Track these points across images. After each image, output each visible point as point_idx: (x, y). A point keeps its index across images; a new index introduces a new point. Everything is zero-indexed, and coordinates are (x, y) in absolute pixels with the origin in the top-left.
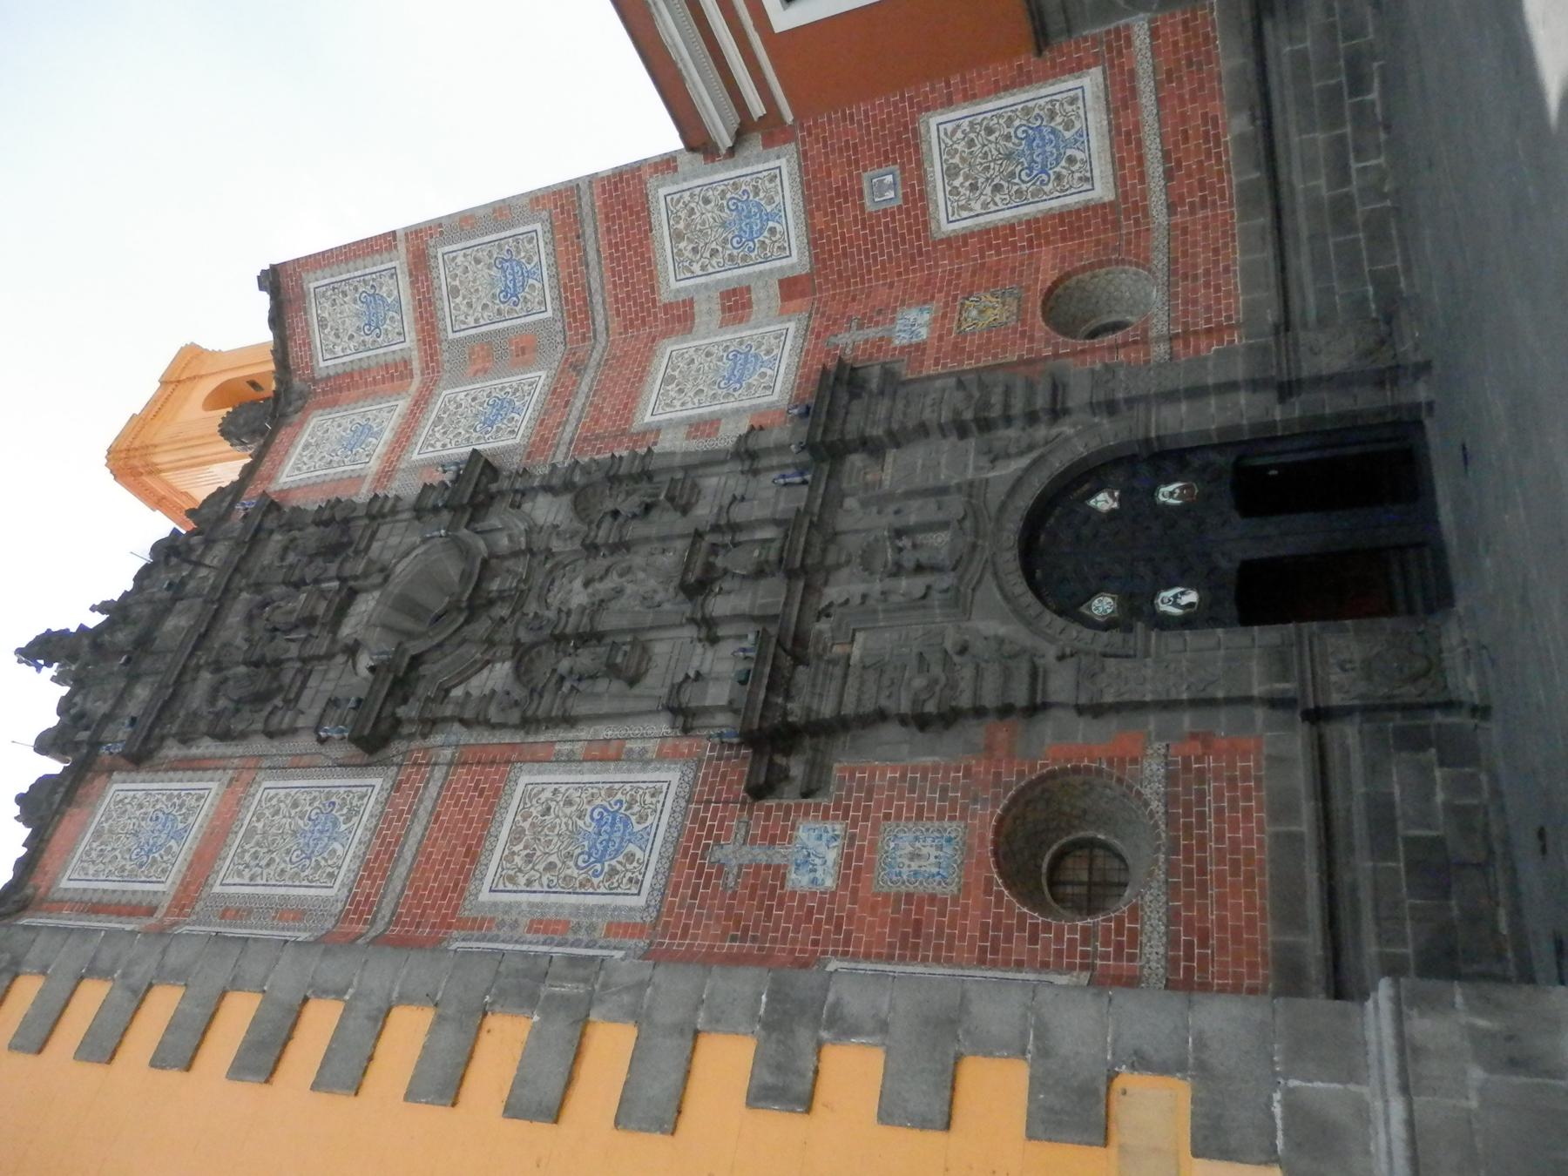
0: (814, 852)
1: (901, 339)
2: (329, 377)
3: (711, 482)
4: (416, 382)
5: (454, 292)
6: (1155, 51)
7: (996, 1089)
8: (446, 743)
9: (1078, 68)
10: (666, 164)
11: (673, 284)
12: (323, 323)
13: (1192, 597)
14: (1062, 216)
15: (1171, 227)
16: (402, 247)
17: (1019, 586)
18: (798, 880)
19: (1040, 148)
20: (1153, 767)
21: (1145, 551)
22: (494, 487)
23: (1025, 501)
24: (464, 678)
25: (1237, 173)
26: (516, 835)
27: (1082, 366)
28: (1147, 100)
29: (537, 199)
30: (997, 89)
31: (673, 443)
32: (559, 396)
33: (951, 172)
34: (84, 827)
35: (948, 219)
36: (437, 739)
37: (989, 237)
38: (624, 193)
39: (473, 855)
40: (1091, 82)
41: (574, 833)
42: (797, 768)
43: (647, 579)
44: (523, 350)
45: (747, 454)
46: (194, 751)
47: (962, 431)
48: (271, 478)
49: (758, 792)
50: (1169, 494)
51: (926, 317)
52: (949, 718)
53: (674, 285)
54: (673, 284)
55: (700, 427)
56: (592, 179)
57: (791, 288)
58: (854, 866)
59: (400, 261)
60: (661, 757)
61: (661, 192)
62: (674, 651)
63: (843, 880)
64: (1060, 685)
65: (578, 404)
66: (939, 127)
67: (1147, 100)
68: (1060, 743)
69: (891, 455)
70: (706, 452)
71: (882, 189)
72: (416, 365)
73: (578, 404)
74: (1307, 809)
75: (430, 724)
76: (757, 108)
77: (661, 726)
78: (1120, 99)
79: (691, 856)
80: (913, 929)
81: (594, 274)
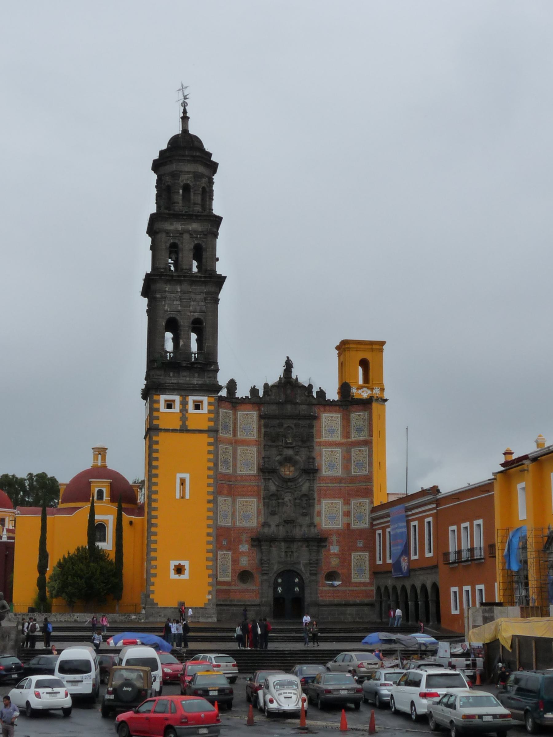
0: (244, 548)
1: (331, 547)
2: (349, 416)
3: (307, 518)
4: (346, 440)
5: (360, 451)
6: (369, 590)
7: (210, 589)
8: (262, 483)
9: (370, 578)
10: (372, 502)
11: (353, 502)
12: (359, 415)
13: (280, 592)
14: (351, 574)
15: (346, 590)
16: (370, 438)
17: (282, 570)
18: (241, 546)
19: (360, 571)
20: (254, 588)
21: (288, 585)
22: (312, 475)
23: (295, 569)
24: (273, 481)
25: (351, 600)
26: (246, 502)
27: (321, 577)
28: (364, 588)
29: (371, 472)
30: (370, 565)
31: (317, 508)
32: (334, 479)
33: (360, 556)
34: (249, 410)
35: (354, 555)
36: (263, 481)
37: (350, 561)
38: (368, 493)
39: (244, 495)
40: (368, 580)
41: (247, 511)
42: (255, 543)
43: (288, 511)
44: (346, 467)
45: (312, 525)
46: (262, 428)
47: (310, 560)
48: (325, 411)
49: (252, 539)
50: (297, 589)
51: (336, 551)
52: (262, 564)
53: (353, 502)
54: (353, 502)
55: (319, 514)
56: (373, 485)
57: (349, 525)
58: (243, 553)
59: (367, 438)
60: (258, 523)
61: (367, 501)
62: (275, 521)
63: (241, 552)
64: (265, 577)
65: (330, 485)
66: (367, 554)
67: (364, 588)
68: (258, 578)
69: (307, 549)
70: (313, 517)
71: (360, 544)
72: (348, 440)
73: (330, 485)
74: (249, 603)
75: (265, 479)
76: (375, 523)
77: (263, 521)
78: (364, 584)
79: (244, 530)
80: (235, 561)
81: (357, 485)
